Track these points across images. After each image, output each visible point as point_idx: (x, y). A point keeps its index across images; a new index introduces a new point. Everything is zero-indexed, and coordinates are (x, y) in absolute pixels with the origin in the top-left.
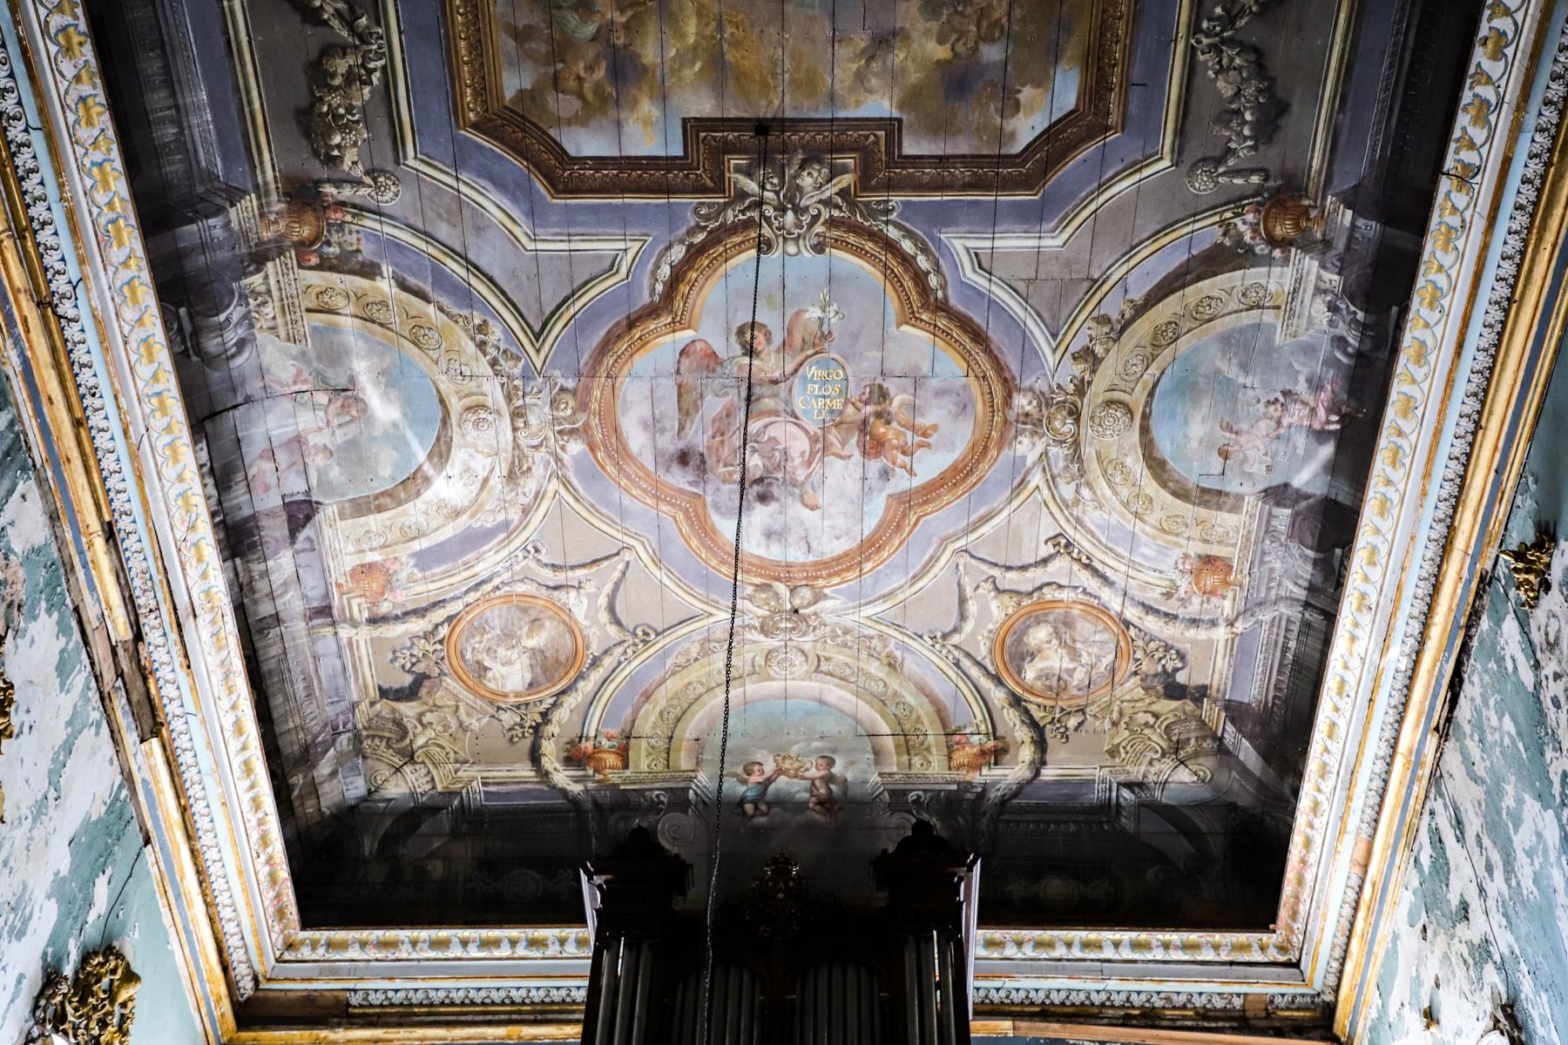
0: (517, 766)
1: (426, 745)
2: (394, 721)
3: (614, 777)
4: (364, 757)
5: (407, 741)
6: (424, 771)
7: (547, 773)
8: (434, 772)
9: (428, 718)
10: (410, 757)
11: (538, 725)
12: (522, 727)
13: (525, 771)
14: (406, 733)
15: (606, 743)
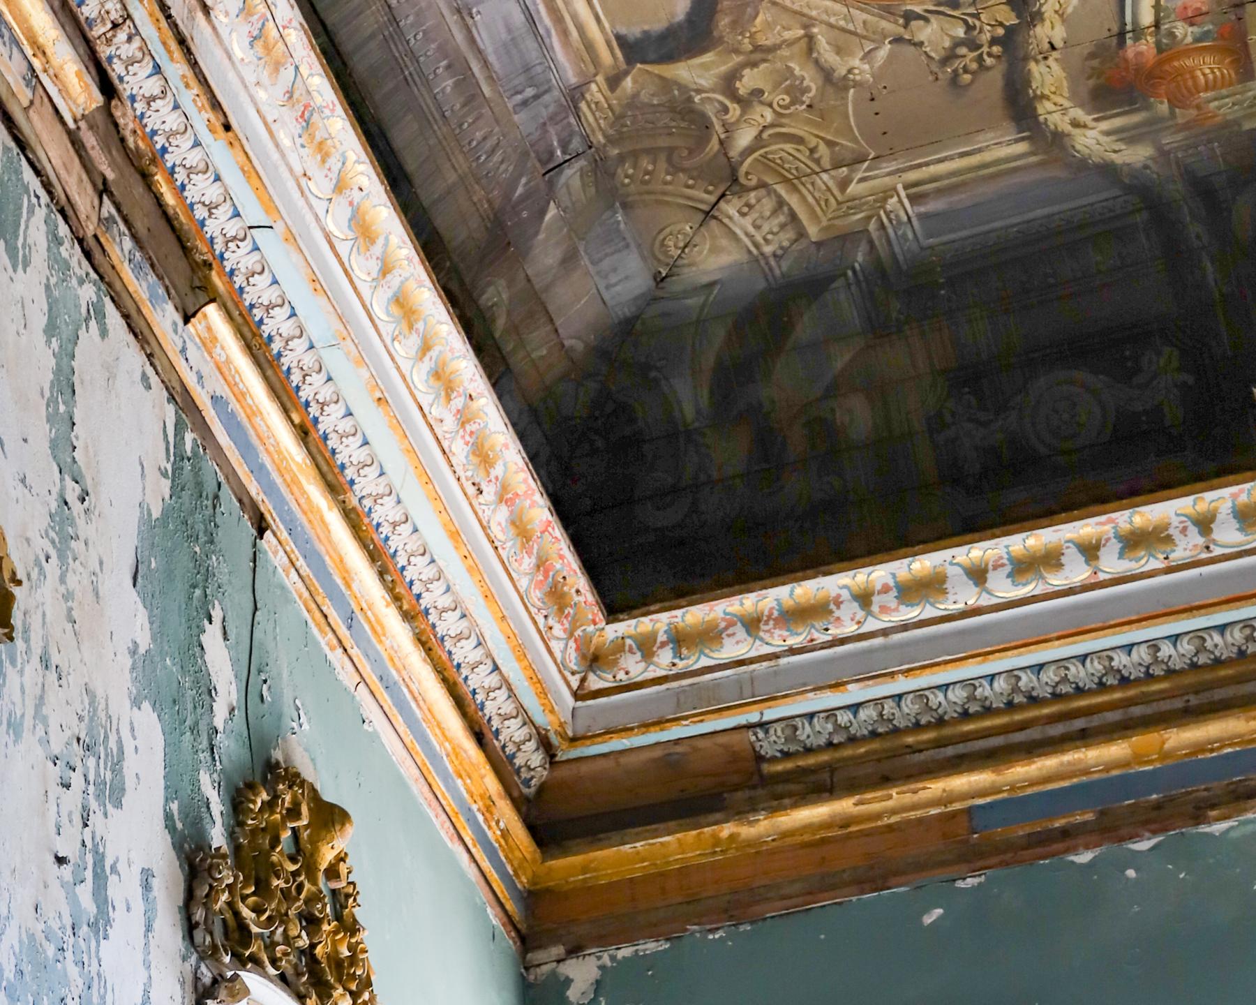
0: (984, 139)
1: (758, 142)
2: (673, 110)
3: (1223, 107)
4: (625, 206)
5: (714, 145)
6: (768, 205)
7: (1058, 138)
8: (793, 201)
9: (749, 81)
10: (730, 180)
11: (1010, 31)
12: (974, 45)
13: (1004, 147)
14: (708, 127)
15: (1181, 29)
